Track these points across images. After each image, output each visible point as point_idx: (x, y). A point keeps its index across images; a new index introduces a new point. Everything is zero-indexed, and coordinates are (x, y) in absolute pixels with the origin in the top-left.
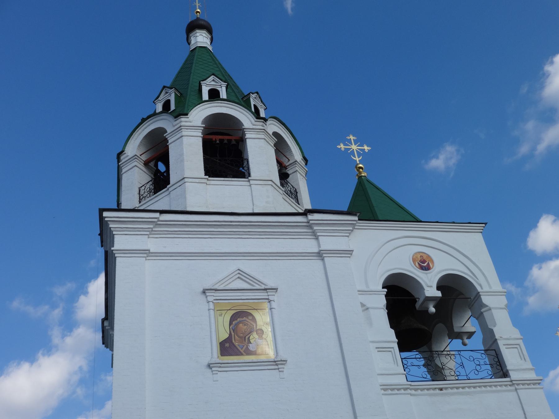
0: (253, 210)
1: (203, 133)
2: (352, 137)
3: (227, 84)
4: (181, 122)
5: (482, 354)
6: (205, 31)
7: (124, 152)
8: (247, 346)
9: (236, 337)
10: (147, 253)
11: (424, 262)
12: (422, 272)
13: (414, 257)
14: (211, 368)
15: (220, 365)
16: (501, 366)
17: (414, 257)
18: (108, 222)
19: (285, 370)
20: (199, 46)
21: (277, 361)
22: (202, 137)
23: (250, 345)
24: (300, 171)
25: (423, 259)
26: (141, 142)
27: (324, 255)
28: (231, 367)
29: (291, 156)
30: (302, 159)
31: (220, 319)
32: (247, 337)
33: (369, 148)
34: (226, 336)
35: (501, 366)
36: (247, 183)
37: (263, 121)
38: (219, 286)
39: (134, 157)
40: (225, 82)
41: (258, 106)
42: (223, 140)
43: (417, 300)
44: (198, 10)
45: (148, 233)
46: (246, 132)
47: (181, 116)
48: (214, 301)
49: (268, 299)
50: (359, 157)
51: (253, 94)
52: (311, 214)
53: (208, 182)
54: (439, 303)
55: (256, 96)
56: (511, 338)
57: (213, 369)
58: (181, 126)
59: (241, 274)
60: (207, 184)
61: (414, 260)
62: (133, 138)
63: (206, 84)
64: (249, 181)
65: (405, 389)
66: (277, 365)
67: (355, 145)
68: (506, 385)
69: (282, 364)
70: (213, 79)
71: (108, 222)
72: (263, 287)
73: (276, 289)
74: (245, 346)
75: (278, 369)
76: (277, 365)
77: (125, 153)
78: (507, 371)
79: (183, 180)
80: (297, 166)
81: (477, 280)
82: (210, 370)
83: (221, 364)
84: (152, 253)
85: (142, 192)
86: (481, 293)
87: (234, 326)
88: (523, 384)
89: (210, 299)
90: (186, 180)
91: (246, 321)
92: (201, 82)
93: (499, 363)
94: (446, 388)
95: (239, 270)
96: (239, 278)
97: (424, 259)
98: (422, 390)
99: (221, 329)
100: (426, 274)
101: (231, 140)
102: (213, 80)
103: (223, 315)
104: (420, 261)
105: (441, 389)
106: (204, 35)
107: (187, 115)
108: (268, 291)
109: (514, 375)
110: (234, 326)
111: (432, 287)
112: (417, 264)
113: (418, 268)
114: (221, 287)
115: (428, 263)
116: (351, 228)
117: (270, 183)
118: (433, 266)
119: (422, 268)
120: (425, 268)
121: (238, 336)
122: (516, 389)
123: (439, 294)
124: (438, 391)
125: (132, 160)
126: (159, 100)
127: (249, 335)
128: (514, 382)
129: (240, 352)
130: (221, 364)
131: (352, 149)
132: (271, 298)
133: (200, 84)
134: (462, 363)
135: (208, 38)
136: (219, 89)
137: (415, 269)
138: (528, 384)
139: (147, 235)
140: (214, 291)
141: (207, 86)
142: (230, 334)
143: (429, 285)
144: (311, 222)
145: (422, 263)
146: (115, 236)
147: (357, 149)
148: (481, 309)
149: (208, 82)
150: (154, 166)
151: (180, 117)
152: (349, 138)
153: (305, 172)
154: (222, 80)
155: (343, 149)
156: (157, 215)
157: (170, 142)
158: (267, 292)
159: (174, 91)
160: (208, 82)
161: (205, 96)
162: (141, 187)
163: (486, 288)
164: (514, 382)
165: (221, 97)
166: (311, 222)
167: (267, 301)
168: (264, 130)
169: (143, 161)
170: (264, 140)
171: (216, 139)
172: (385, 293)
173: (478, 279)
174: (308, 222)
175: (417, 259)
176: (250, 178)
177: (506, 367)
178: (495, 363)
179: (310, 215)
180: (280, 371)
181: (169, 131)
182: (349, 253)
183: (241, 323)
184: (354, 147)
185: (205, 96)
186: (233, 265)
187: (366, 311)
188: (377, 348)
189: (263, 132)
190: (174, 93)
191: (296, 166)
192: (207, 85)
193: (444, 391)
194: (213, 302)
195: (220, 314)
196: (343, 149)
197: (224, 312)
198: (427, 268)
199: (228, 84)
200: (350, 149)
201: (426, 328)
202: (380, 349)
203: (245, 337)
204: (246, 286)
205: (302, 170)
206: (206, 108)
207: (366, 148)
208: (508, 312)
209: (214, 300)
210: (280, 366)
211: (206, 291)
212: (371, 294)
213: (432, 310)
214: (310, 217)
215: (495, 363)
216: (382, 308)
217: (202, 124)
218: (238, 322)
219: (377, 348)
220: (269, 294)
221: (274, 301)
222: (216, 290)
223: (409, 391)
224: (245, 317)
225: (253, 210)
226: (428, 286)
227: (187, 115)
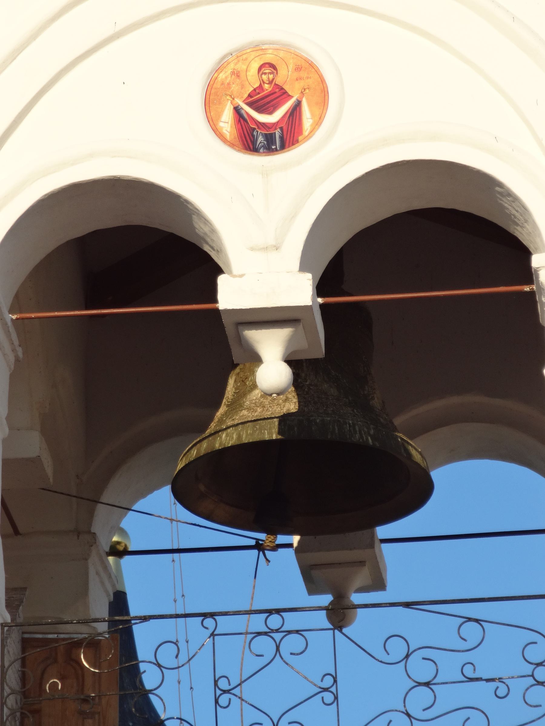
5: (470, 619)
13: (222, 76)
25: (270, 82)
97: (279, 80)
104: (250, 96)
113: (232, 145)
115: (298, 105)
118: (318, 123)
120: (270, 139)
175: (235, 88)
178: (528, 669)
215: (528, 669)
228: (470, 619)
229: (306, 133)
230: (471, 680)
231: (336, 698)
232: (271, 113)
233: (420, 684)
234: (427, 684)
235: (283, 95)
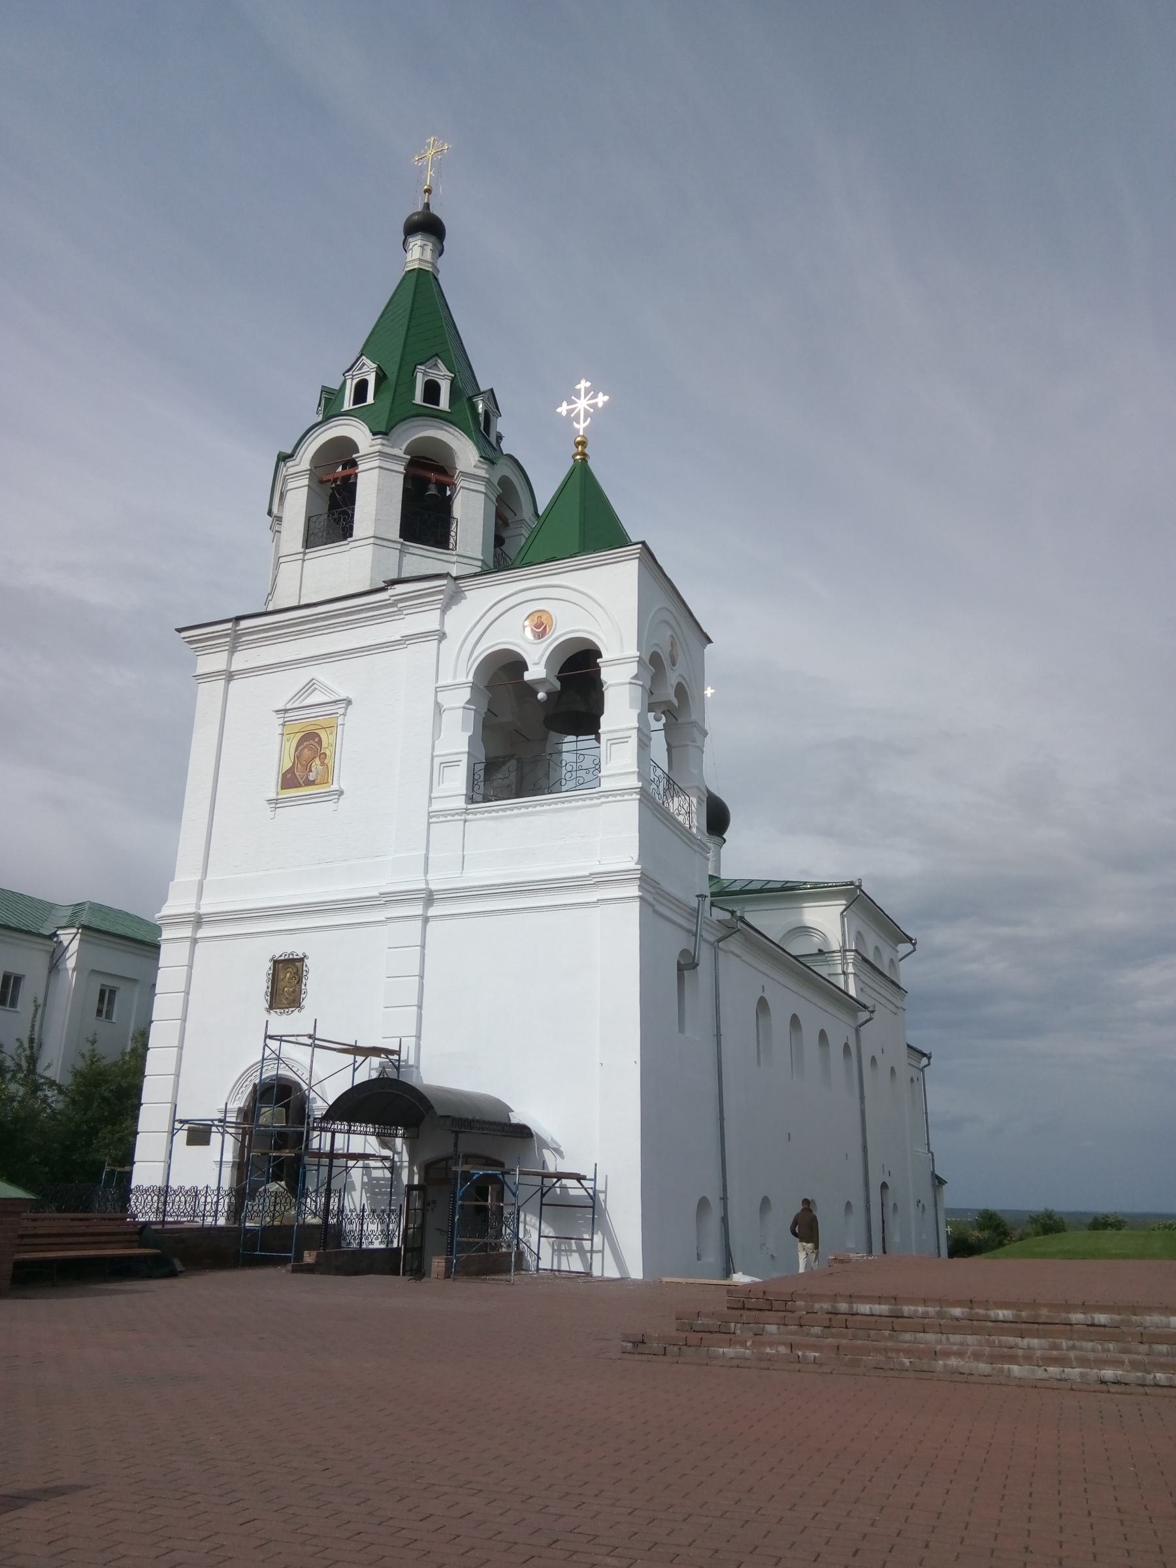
23: (311, 773)
24: (473, 486)
28: (290, 801)
30: (479, 461)
33: (606, 398)
34: (290, 765)
46: (358, 463)
49: (337, 713)
51: (420, 364)
63: (351, 376)
103: (291, 740)
109: (606, 785)
114: (296, 705)
129: (300, 783)
138: (622, 795)
176: (349, 539)
186: (302, 676)
200: (573, 412)
207: (602, 399)
232: (539, 629)
235: (543, 624)
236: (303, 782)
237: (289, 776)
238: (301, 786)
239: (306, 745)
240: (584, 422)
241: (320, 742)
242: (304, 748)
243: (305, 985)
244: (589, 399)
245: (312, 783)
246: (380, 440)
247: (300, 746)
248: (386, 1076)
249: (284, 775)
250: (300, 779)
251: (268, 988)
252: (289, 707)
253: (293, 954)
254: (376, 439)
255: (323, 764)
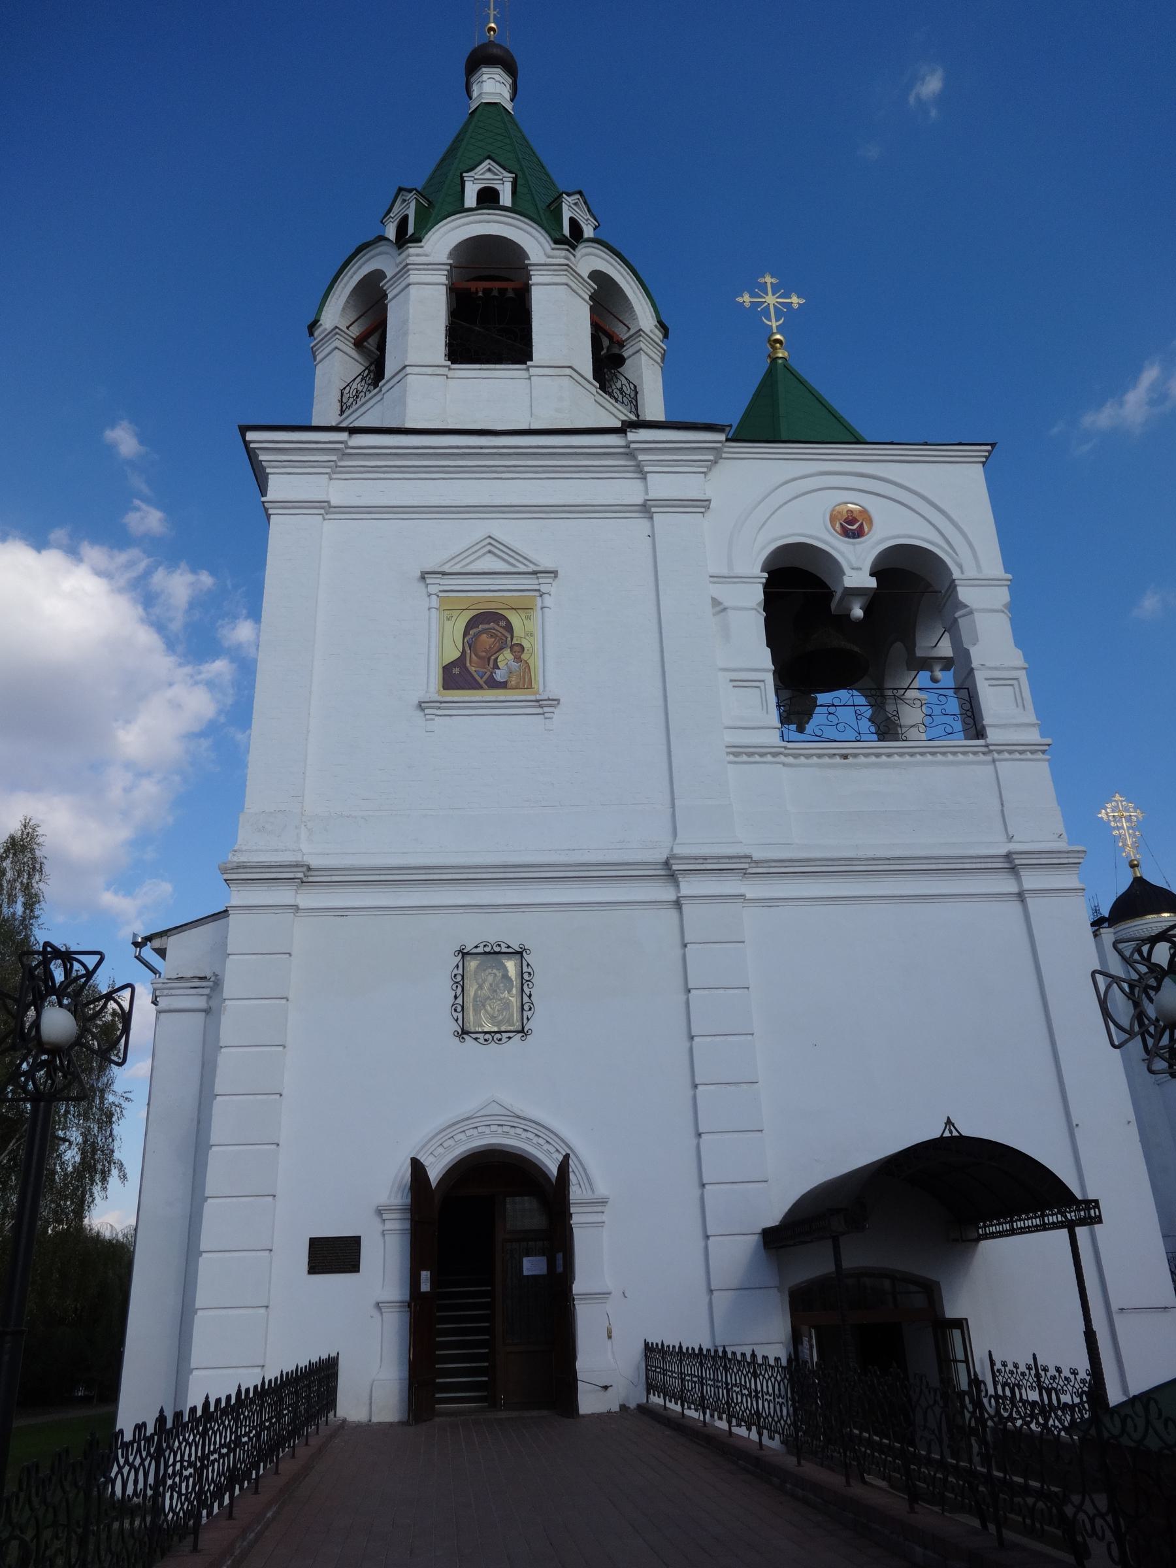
0: (530, 424)
1: (450, 276)
2: (769, 280)
3: (514, 175)
4: (409, 256)
5: (941, 695)
6: (499, 70)
7: (319, 324)
8: (492, 673)
9: (473, 656)
10: (325, 508)
11: (852, 521)
12: (848, 543)
14: (423, 710)
15: (438, 704)
16: (974, 719)
17: (834, 513)
18: (256, 450)
19: (555, 716)
20: (485, 103)
21: (542, 700)
22: (446, 285)
23: (497, 671)
24: (649, 352)
25: (852, 516)
26: (347, 302)
27: (653, 510)
28: (459, 708)
29: (634, 320)
30: (656, 326)
31: (449, 625)
32: (493, 658)
33: (802, 301)
34: (456, 655)
35: (974, 719)
36: (524, 374)
37: (567, 247)
38: (452, 566)
39: (334, 332)
40: (510, 172)
41: (580, 221)
42: (491, 290)
43: (834, 593)
44: (493, 25)
45: (328, 470)
47: (409, 245)
48: (441, 594)
49: (539, 590)
50: (777, 321)
51: (569, 195)
52: (634, 430)
53: (451, 373)
54: (874, 601)
55: (578, 199)
56: (1003, 666)
57: (427, 711)
58: (408, 264)
59: (493, 545)
60: (447, 378)
61: (833, 519)
62: (334, 293)
63: (473, 179)
64: (527, 369)
65: (775, 755)
66: (541, 706)
67: (773, 295)
68: (975, 753)
69: (550, 706)
70: (489, 166)
71: (256, 450)
72: (532, 568)
73: (554, 573)
74: (488, 673)
75: (543, 714)
76: (542, 707)
77: (321, 325)
78: (984, 727)
79: (404, 371)
80: (642, 339)
81: (956, 557)
82: (422, 714)
83: (441, 702)
84: (335, 507)
85: (346, 396)
86: (957, 582)
87: (472, 638)
88: (1010, 752)
89: (433, 589)
90: (409, 370)
91: (494, 629)
92: (464, 174)
93: (973, 712)
94: (855, 756)
95: (490, 537)
96: (490, 552)
98: (808, 756)
99: (448, 642)
100: (854, 544)
101: (507, 289)
102: (489, 170)
104: (845, 520)
105: (845, 757)
106: (497, 77)
107: (421, 241)
108: (538, 575)
110: (472, 638)
111: (860, 569)
112: (838, 525)
114: (457, 569)
115: (862, 524)
116: (711, 458)
117: (568, 371)
118: (869, 531)
119: (847, 533)
120: (854, 534)
121: (476, 655)
122: (994, 761)
123: (872, 583)
124: (838, 760)
125: (332, 338)
126: (391, 217)
127: (497, 655)
128: (991, 748)
129: (478, 683)
130: (441, 702)
131: (766, 304)
132: (544, 589)
133: (462, 178)
134: (898, 712)
135: (505, 83)
136: (498, 187)
137: (833, 536)
138: (1021, 752)
139: (327, 474)
140: (440, 576)
141: (475, 181)
142: (463, 652)
143: (855, 566)
144: (632, 445)
145: (849, 525)
146: (270, 476)
147: (776, 304)
148: (955, 612)
149: (479, 174)
150: (377, 349)
151: (405, 247)
152: (762, 280)
153: (660, 352)
154: (504, 169)
155: (747, 305)
156: (343, 436)
157: (390, 296)
158: (538, 578)
159: (415, 196)
160: (479, 174)
161: (470, 200)
162: (345, 388)
163: (971, 572)
164: (991, 748)
165: (501, 203)
166: (632, 445)
167: (537, 594)
168: (566, 267)
169: (353, 338)
170: (566, 286)
171: (477, 289)
172: (764, 580)
173: (957, 555)
174: (628, 447)
176: (529, 363)
177: (982, 719)
179: (631, 432)
180: (546, 718)
181: (389, 275)
182: (703, 505)
183: (484, 633)
184: (771, 299)
185: (470, 200)
186: (478, 529)
187: (722, 614)
188: (731, 681)
189: (566, 270)
190: (415, 200)
191: (640, 341)
192: (475, 179)
193: (851, 760)
194: (438, 596)
195: (448, 617)
196: (747, 305)
197: (456, 613)
198: (858, 534)
199: (516, 175)
201: (856, 649)
202: (739, 684)
203: (489, 659)
204: (501, 566)
205: (655, 348)
206: (460, 227)
207: (795, 300)
208: (1010, 619)
209: (440, 591)
210: (546, 709)
211: (426, 576)
212: (735, 583)
213: (858, 612)
214: (632, 436)
216: (753, 609)
217: (448, 258)
218: (480, 631)
219: (731, 681)
220: (541, 581)
221: (550, 595)
222: (444, 574)
223: (782, 758)
224: (493, 622)
225: (530, 424)
226: (853, 569)
227: (420, 241)
228: (941, 695)
229: (866, 532)
230: (945, 714)
231: (899, 718)
232: (853, 526)
233: (927, 715)
234: (930, 715)
236: (485, 682)
237: (456, 671)
238: (481, 688)
239: (484, 630)
240: (777, 321)
241: (509, 627)
242: (480, 633)
243: (530, 996)
244: (777, 298)
245: (503, 685)
246: (564, 252)
247: (472, 628)
248: (955, 1134)
249: (447, 670)
250: (478, 678)
251: (456, 997)
252: (446, 569)
253: (499, 945)
254: (558, 249)
255: (518, 659)
